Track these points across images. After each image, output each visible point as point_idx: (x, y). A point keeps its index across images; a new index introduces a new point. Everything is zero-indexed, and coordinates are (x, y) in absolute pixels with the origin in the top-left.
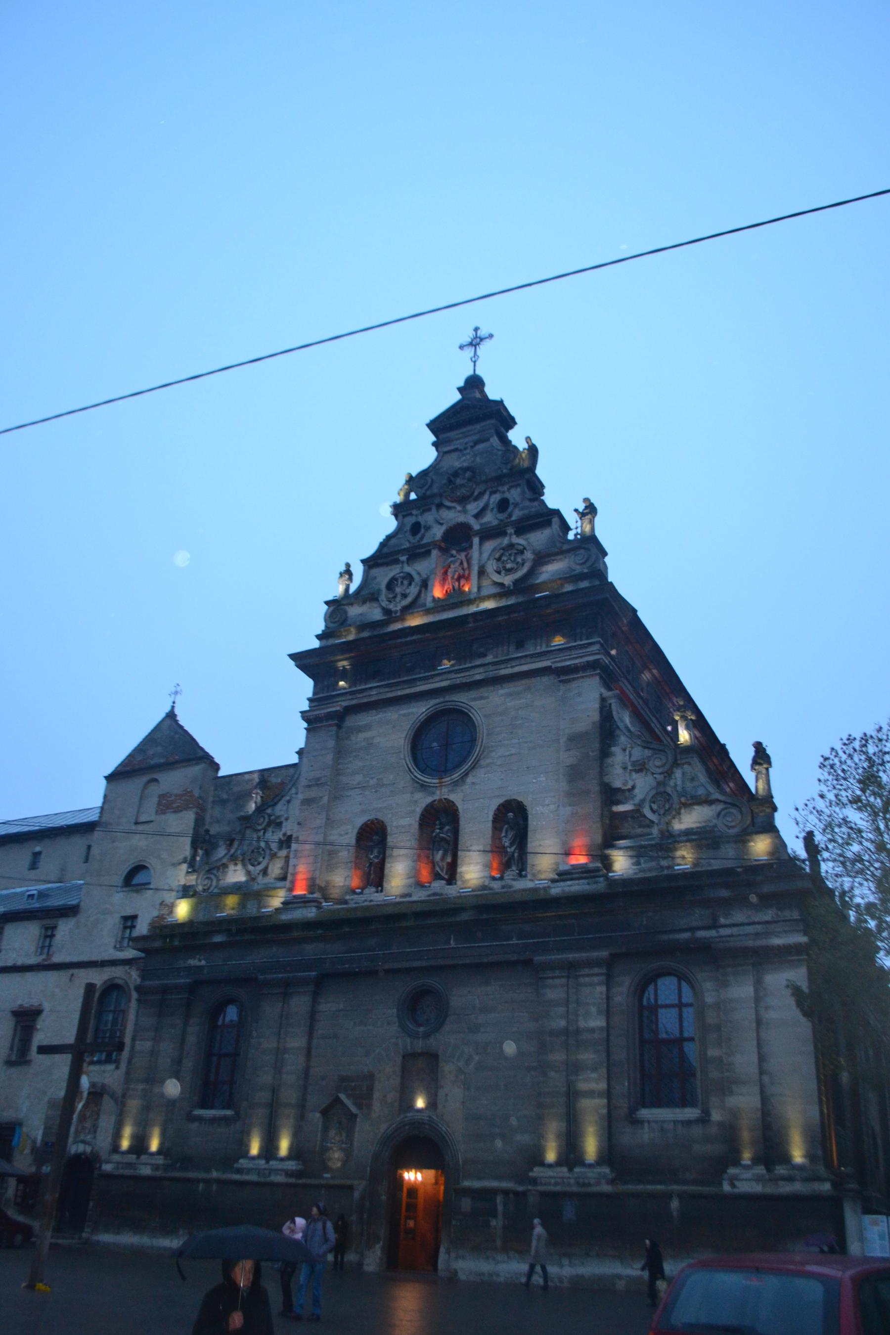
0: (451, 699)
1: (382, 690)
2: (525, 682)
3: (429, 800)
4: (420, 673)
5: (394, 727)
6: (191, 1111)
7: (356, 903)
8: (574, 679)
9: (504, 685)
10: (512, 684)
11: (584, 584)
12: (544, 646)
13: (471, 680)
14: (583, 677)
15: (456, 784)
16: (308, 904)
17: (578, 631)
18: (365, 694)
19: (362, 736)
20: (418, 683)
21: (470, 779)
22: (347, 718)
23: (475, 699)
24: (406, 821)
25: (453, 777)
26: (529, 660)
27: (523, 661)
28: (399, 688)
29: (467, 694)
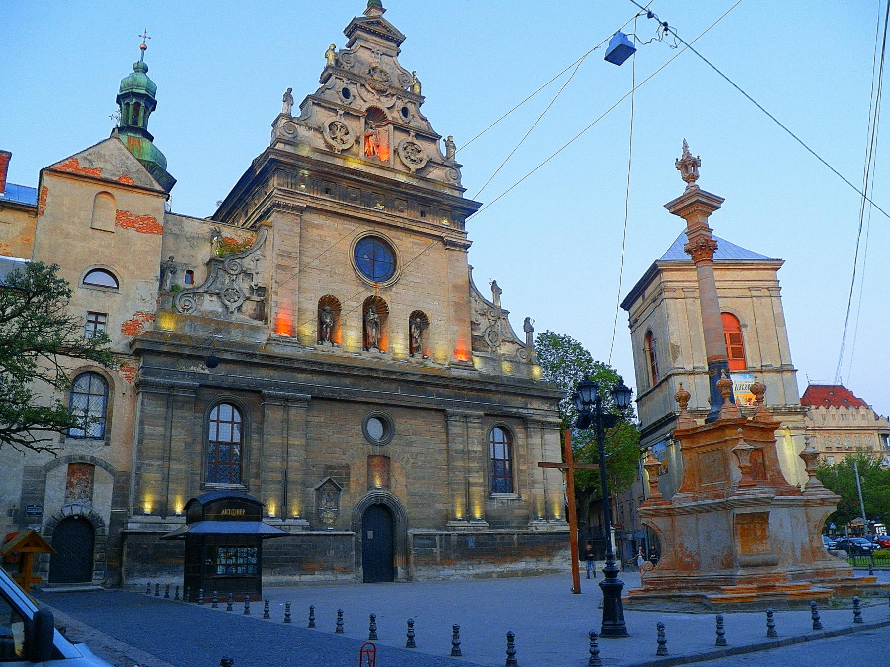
0: (379, 231)
1: (335, 205)
2: (424, 238)
3: (369, 295)
4: (361, 205)
5: (340, 234)
6: (204, 484)
7: (323, 351)
8: (455, 250)
9: (412, 236)
10: (416, 237)
11: (456, 193)
12: (438, 222)
13: (395, 225)
14: (460, 251)
15: (385, 289)
16: (290, 344)
17: (456, 222)
18: (321, 202)
19: (315, 230)
20: (360, 212)
21: (394, 289)
22: (304, 213)
23: (394, 237)
24: (355, 304)
25: (385, 284)
26: (429, 227)
27: (426, 226)
28: (346, 208)
29: (389, 232)
